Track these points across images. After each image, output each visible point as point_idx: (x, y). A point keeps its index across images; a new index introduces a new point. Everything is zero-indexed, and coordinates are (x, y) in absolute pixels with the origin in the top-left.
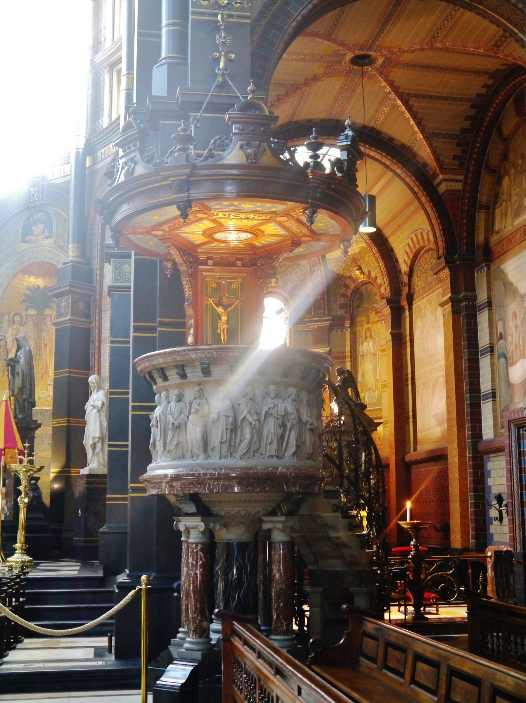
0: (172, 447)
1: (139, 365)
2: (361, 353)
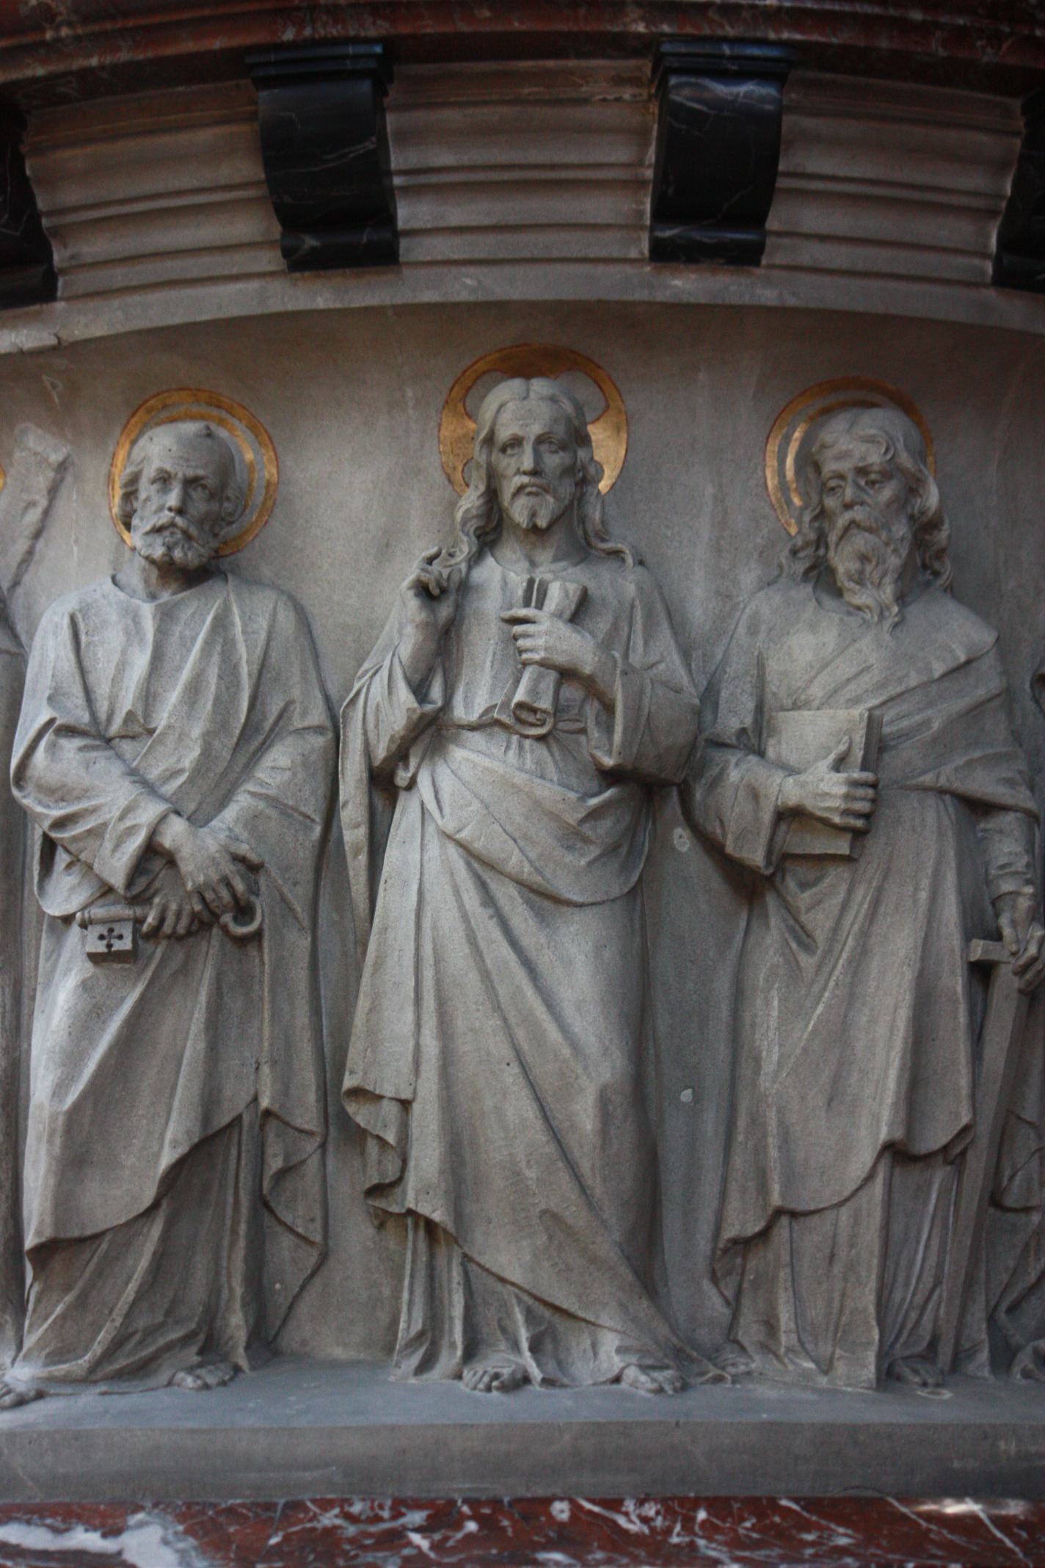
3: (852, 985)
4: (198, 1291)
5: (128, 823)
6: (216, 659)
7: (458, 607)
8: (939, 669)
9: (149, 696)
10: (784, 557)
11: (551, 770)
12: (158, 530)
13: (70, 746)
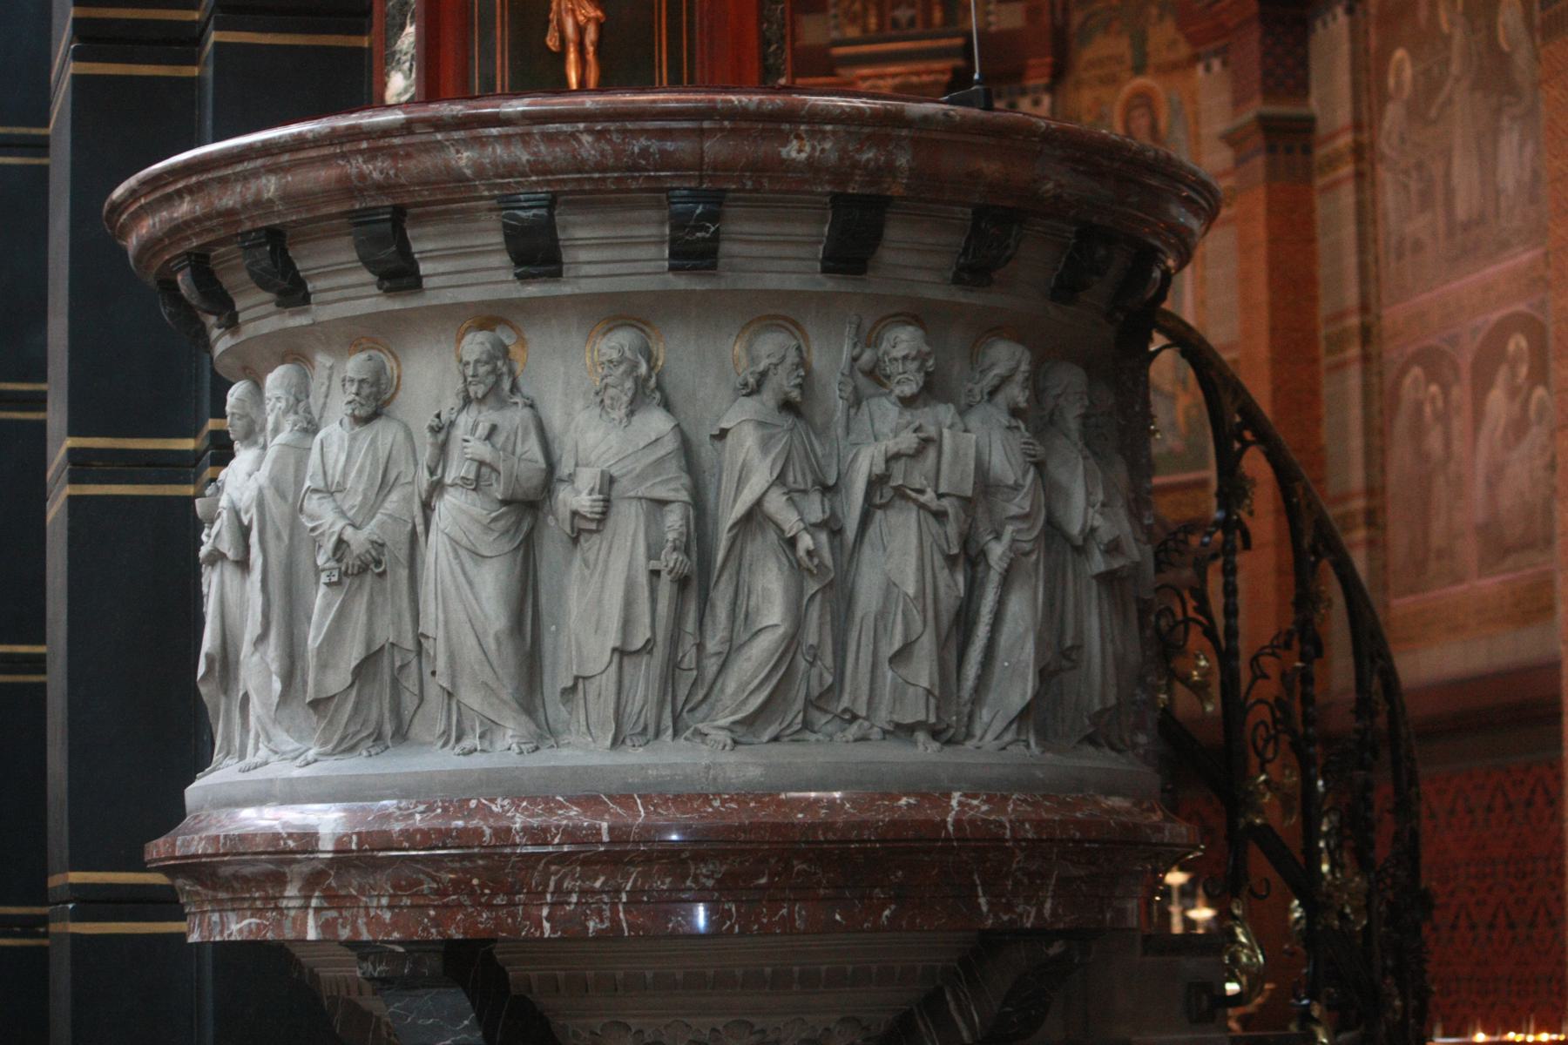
0: (338, 680)
1: (137, 217)
3: (603, 583)
4: (374, 716)
5: (331, 530)
6: (370, 457)
7: (448, 433)
8: (642, 445)
9: (345, 474)
10: (592, 396)
11: (478, 502)
12: (350, 402)
13: (316, 496)
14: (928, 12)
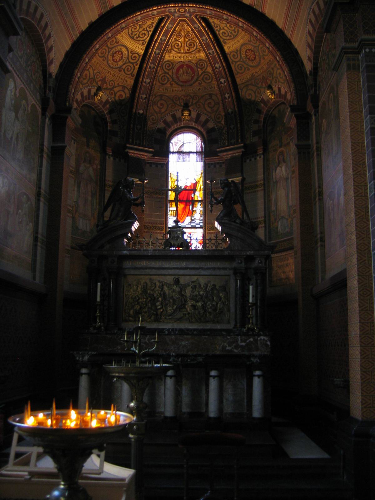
2: (274, 180)
14: (238, 140)
